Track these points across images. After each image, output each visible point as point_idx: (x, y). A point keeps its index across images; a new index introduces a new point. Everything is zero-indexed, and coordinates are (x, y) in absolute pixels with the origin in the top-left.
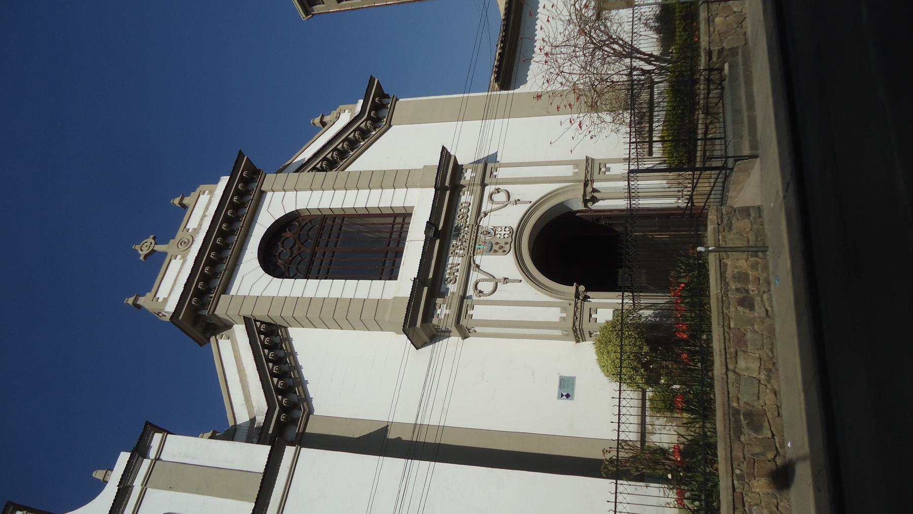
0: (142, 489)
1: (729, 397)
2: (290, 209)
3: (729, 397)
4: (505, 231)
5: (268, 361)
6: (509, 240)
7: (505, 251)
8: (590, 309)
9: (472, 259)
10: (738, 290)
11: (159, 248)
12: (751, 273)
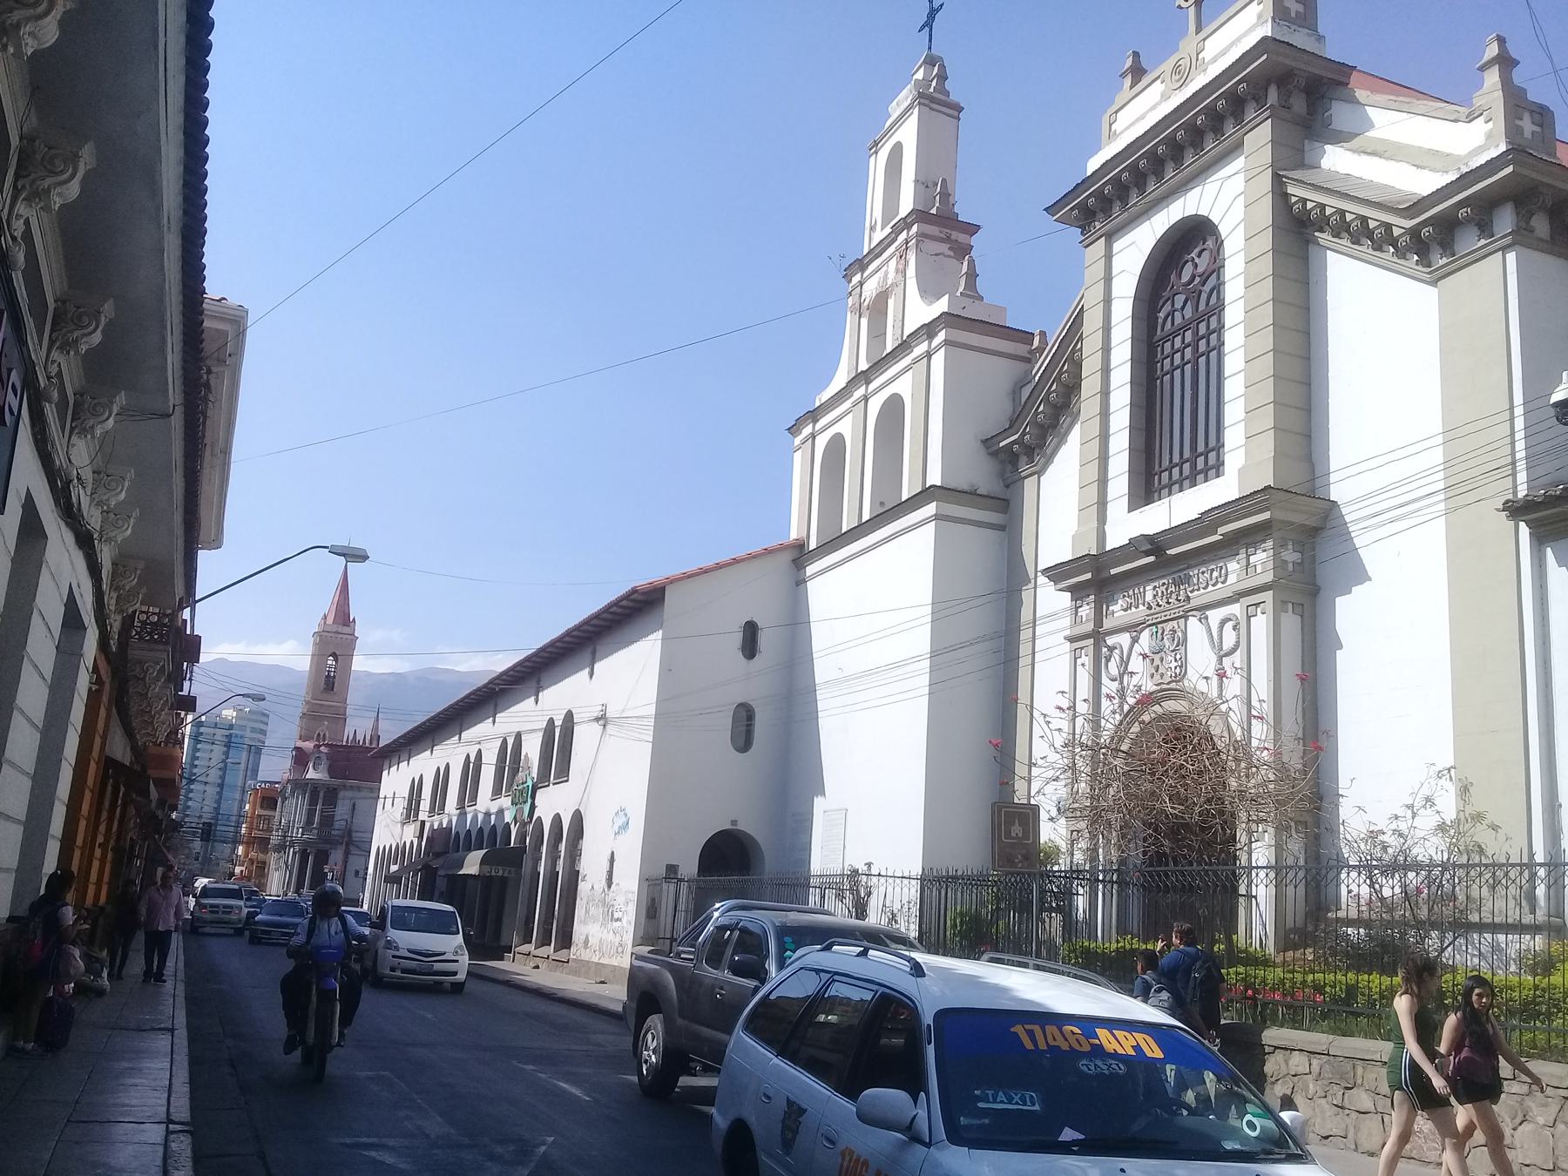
2: (1223, 230)
4: (1176, 668)
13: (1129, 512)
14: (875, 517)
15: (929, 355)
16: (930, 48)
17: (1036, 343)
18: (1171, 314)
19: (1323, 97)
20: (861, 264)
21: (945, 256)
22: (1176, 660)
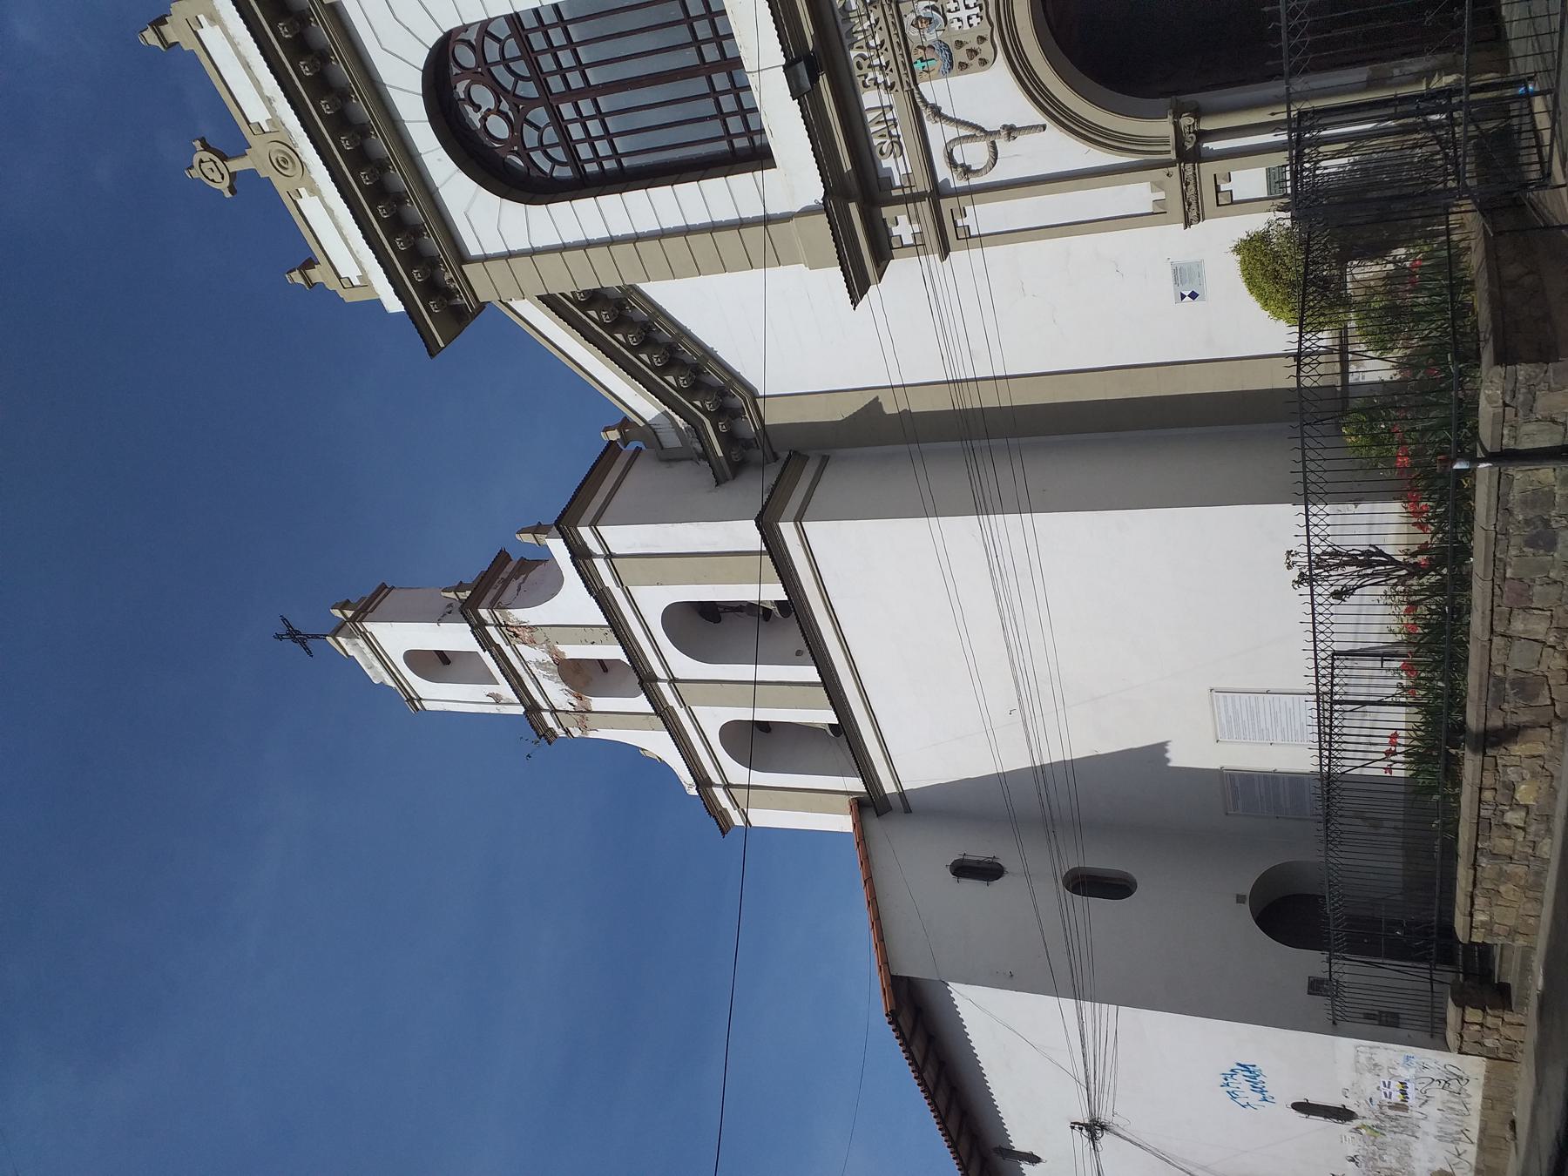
0: (623, 590)
1: (1490, 665)
2: (433, 36)
3: (1490, 665)
4: (967, 7)
5: (635, 350)
7: (983, 62)
8: (1215, 175)
9: (917, 96)
10: (1527, 522)
11: (235, 165)
12: (1560, 492)
13: (775, 167)
14: (815, 662)
15: (609, 556)
16: (326, 636)
17: (614, 435)
18: (542, 147)
20: (532, 709)
21: (523, 582)
22: (957, 10)
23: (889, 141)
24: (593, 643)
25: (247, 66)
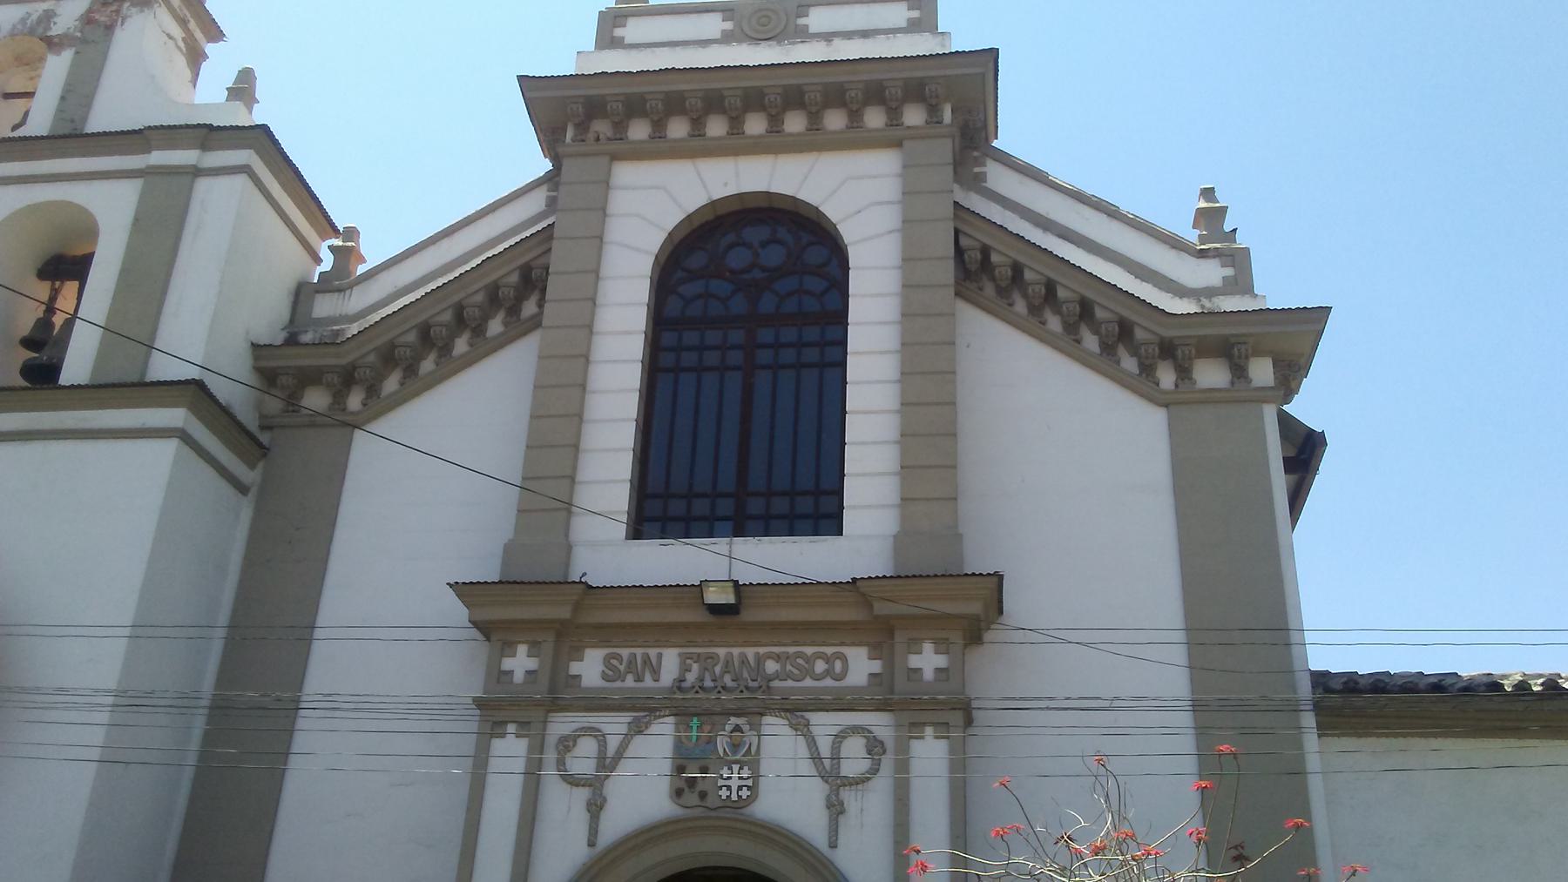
4: (740, 788)
6: (710, 802)
7: (678, 793)
15: (197, 172)
19: (975, 149)
21: (176, 44)
23: (622, 668)
24: (63, 98)
25: (865, 34)
